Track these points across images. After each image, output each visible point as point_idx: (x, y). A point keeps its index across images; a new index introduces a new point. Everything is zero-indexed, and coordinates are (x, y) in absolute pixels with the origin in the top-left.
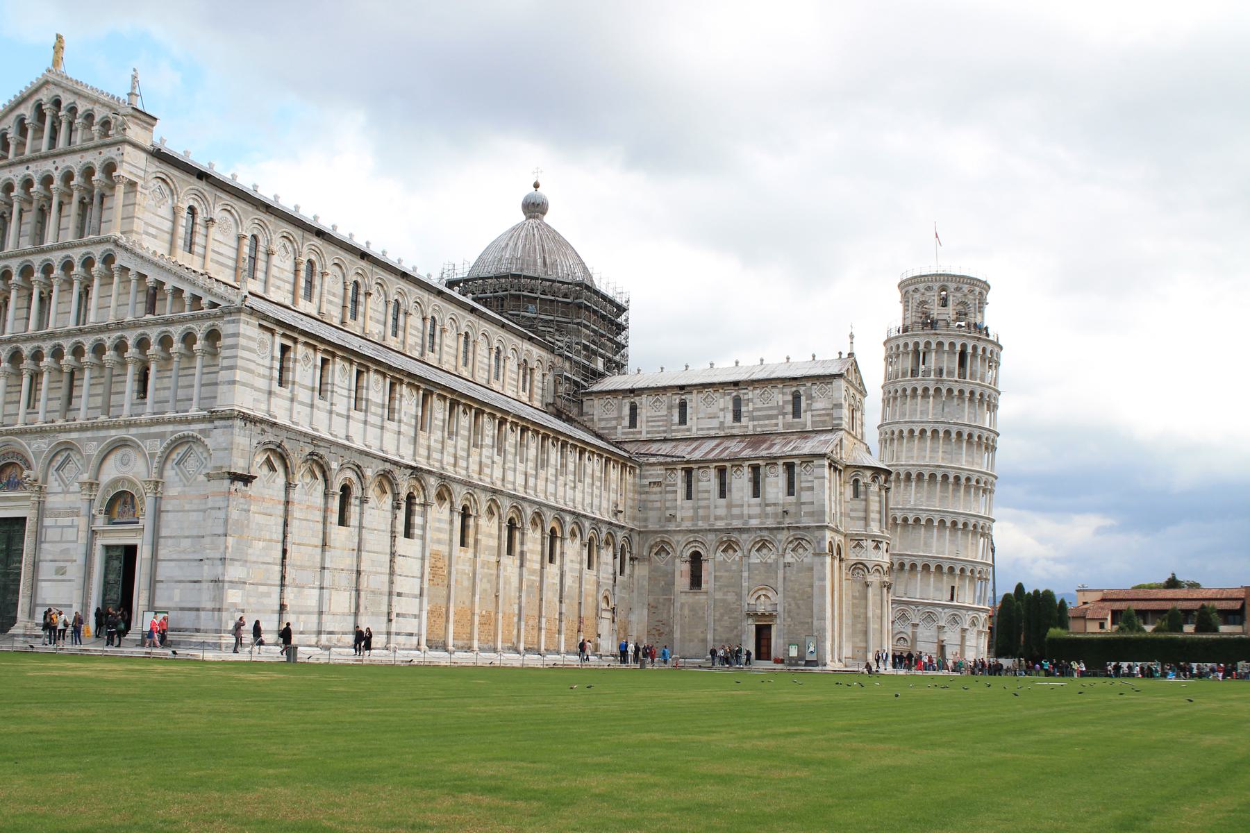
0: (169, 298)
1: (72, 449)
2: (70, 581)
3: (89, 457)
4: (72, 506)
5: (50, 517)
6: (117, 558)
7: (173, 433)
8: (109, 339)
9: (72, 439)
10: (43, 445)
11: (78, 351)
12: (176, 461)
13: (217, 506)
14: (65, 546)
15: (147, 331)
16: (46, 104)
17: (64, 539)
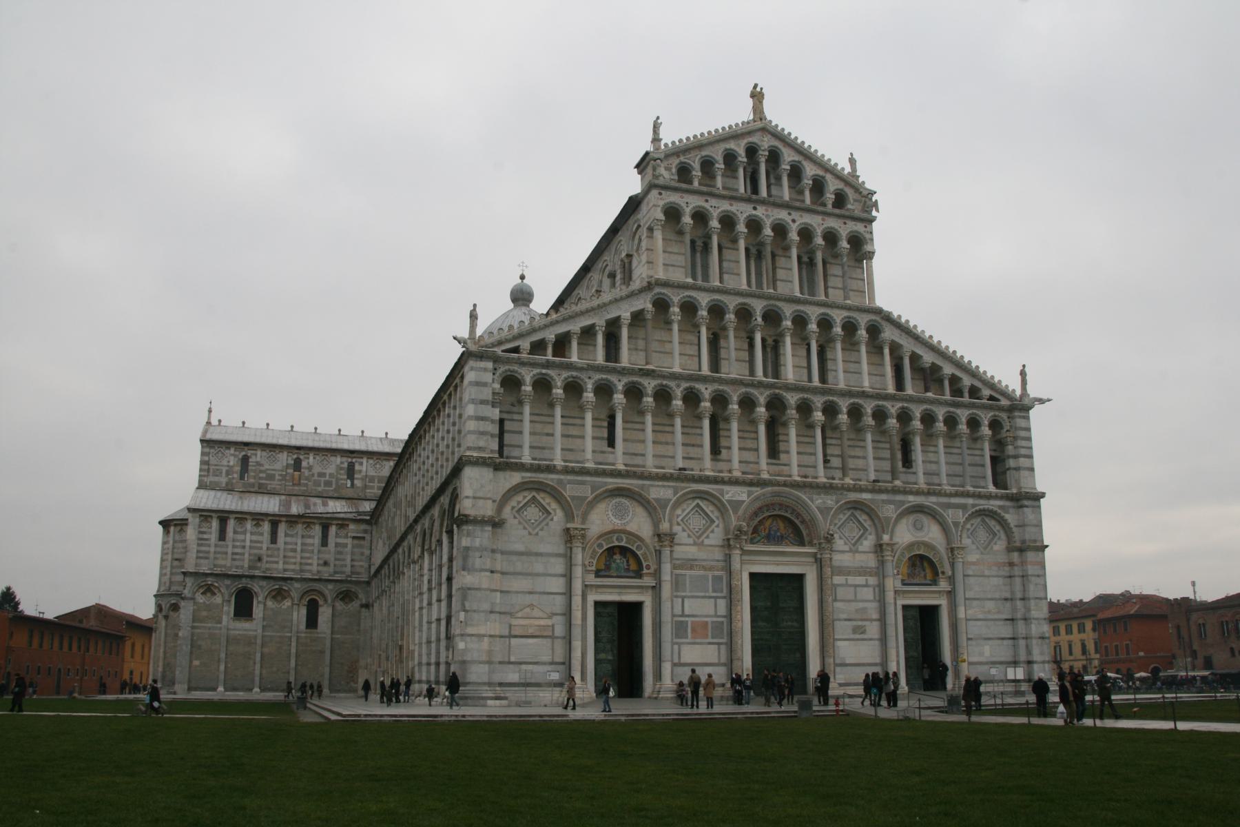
0: (946, 383)
1: (855, 508)
2: (871, 639)
3: (888, 519)
4: (863, 565)
5: (837, 575)
7: (974, 506)
8: (893, 408)
9: (865, 499)
10: (829, 502)
11: (855, 413)
12: (970, 531)
13: (1036, 573)
14: (861, 605)
15: (934, 408)
16: (763, 150)
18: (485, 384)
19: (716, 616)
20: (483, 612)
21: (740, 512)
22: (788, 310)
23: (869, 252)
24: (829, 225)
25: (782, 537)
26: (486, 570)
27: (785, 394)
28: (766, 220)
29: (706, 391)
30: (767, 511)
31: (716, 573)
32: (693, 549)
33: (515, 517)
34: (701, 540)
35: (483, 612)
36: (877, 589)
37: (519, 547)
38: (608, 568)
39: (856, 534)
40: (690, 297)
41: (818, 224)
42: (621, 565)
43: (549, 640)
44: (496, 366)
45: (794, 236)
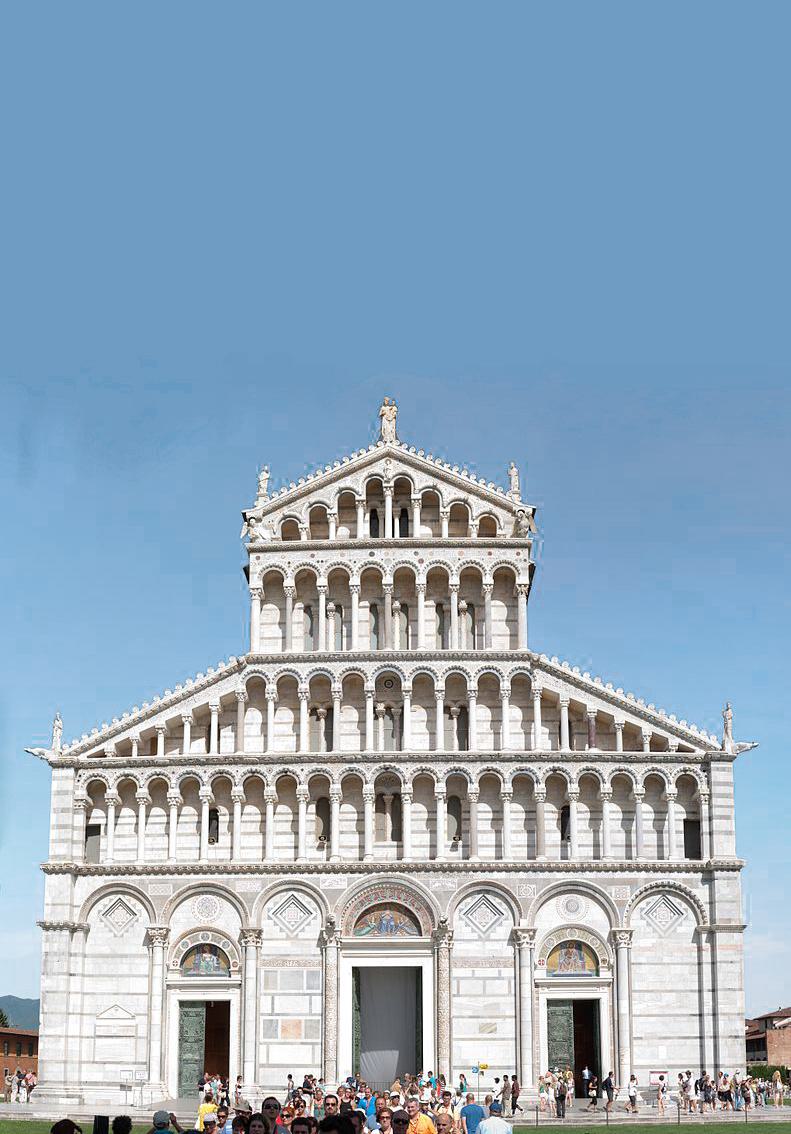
0: (620, 735)
1: (488, 892)
2: (503, 1039)
6: (564, 1013)
7: (647, 880)
9: (497, 880)
10: (450, 884)
11: (490, 782)
14: (492, 1000)
17: (487, 992)
18: (66, 793)
19: (311, 1014)
20: (60, 1013)
21: (340, 901)
22: (408, 669)
23: (520, 585)
24: (469, 560)
25: (397, 926)
26: (63, 974)
27: (397, 766)
28: (385, 566)
29: (303, 773)
30: (375, 899)
31: (312, 969)
32: (287, 944)
33: (102, 921)
34: (295, 933)
35: (60, 1013)
36: (513, 981)
37: (106, 950)
38: (197, 966)
39: (491, 917)
40: (288, 670)
41: (454, 561)
42: (211, 963)
43: (133, 1040)
44: (80, 772)
45: (421, 580)
